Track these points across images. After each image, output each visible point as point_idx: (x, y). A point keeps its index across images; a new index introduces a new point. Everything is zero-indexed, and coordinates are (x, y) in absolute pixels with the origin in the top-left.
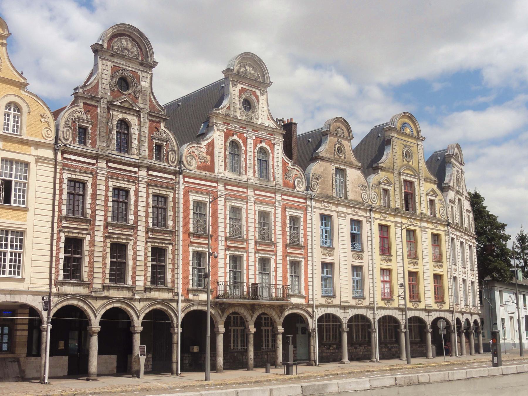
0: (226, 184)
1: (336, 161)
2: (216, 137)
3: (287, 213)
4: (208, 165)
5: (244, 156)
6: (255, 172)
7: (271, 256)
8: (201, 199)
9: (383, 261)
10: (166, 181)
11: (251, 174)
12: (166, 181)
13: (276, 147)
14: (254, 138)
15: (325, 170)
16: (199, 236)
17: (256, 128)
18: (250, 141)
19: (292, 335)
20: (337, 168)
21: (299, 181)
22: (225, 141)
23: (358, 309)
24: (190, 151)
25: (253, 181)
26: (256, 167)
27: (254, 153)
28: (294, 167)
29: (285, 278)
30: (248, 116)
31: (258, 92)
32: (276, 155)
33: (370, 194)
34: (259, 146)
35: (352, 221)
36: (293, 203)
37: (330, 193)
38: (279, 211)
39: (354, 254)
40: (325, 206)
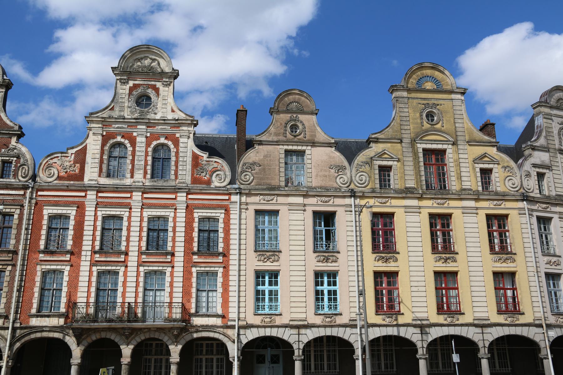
0: (98, 192)
1: (288, 142)
2: (89, 143)
3: (196, 215)
4: (76, 174)
5: (131, 158)
6: (145, 173)
7: (164, 268)
8: (60, 212)
9: (380, 262)
10: (11, 198)
11: (139, 176)
12: (11, 198)
13: (181, 140)
14: (148, 135)
15: (265, 156)
16: (52, 253)
17: (150, 124)
18: (141, 140)
19: (113, 367)
20: (287, 152)
21: (217, 175)
22: (103, 145)
23: (325, 328)
24: (51, 161)
25: (141, 184)
26: (149, 168)
27: (147, 152)
28: (211, 159)
29: (186, 293)
30: (141, 113)
31: (159, 85)
32: (181, 149)
33: (353, 176)
34: (155, 143)
35: (316, 214)
36: (201, 202)
37: (275, 182)
38: (181, 214)
39: (318, 256)
40: (264, 200)
